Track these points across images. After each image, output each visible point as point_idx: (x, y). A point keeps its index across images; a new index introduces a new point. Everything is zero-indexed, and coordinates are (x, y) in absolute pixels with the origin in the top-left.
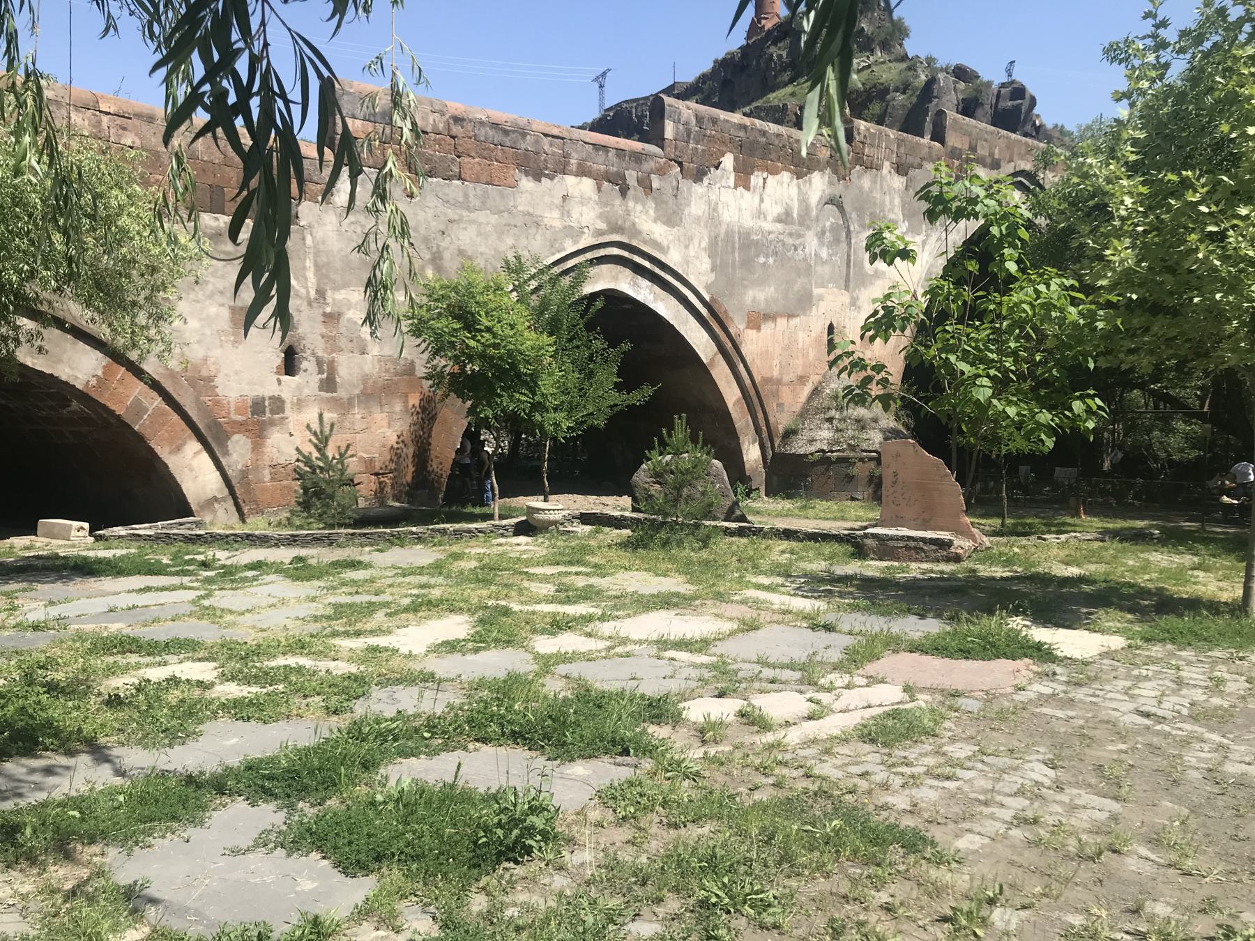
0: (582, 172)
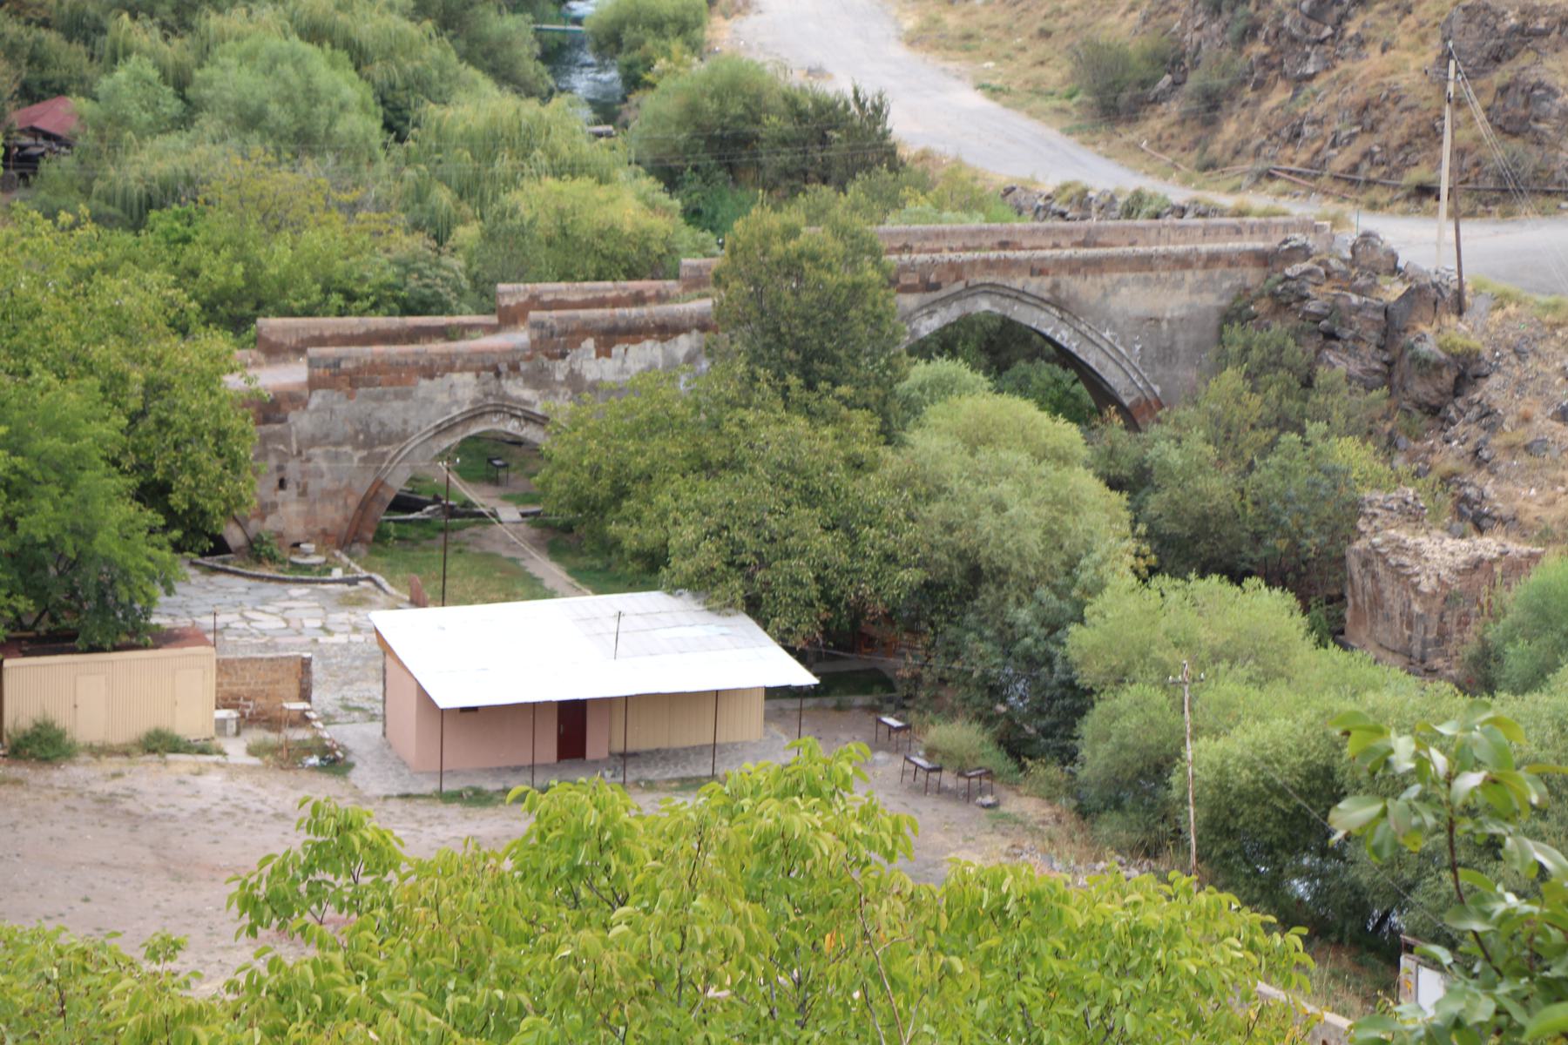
0: (462, 370)
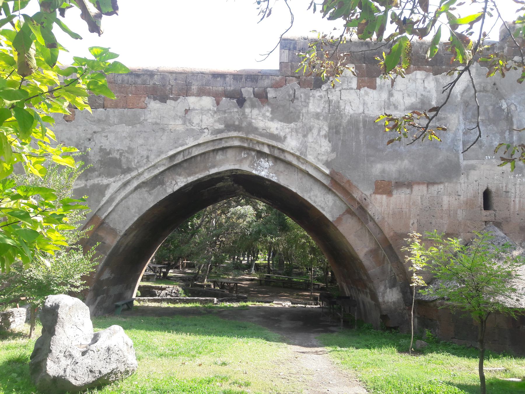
0: (201, 93)
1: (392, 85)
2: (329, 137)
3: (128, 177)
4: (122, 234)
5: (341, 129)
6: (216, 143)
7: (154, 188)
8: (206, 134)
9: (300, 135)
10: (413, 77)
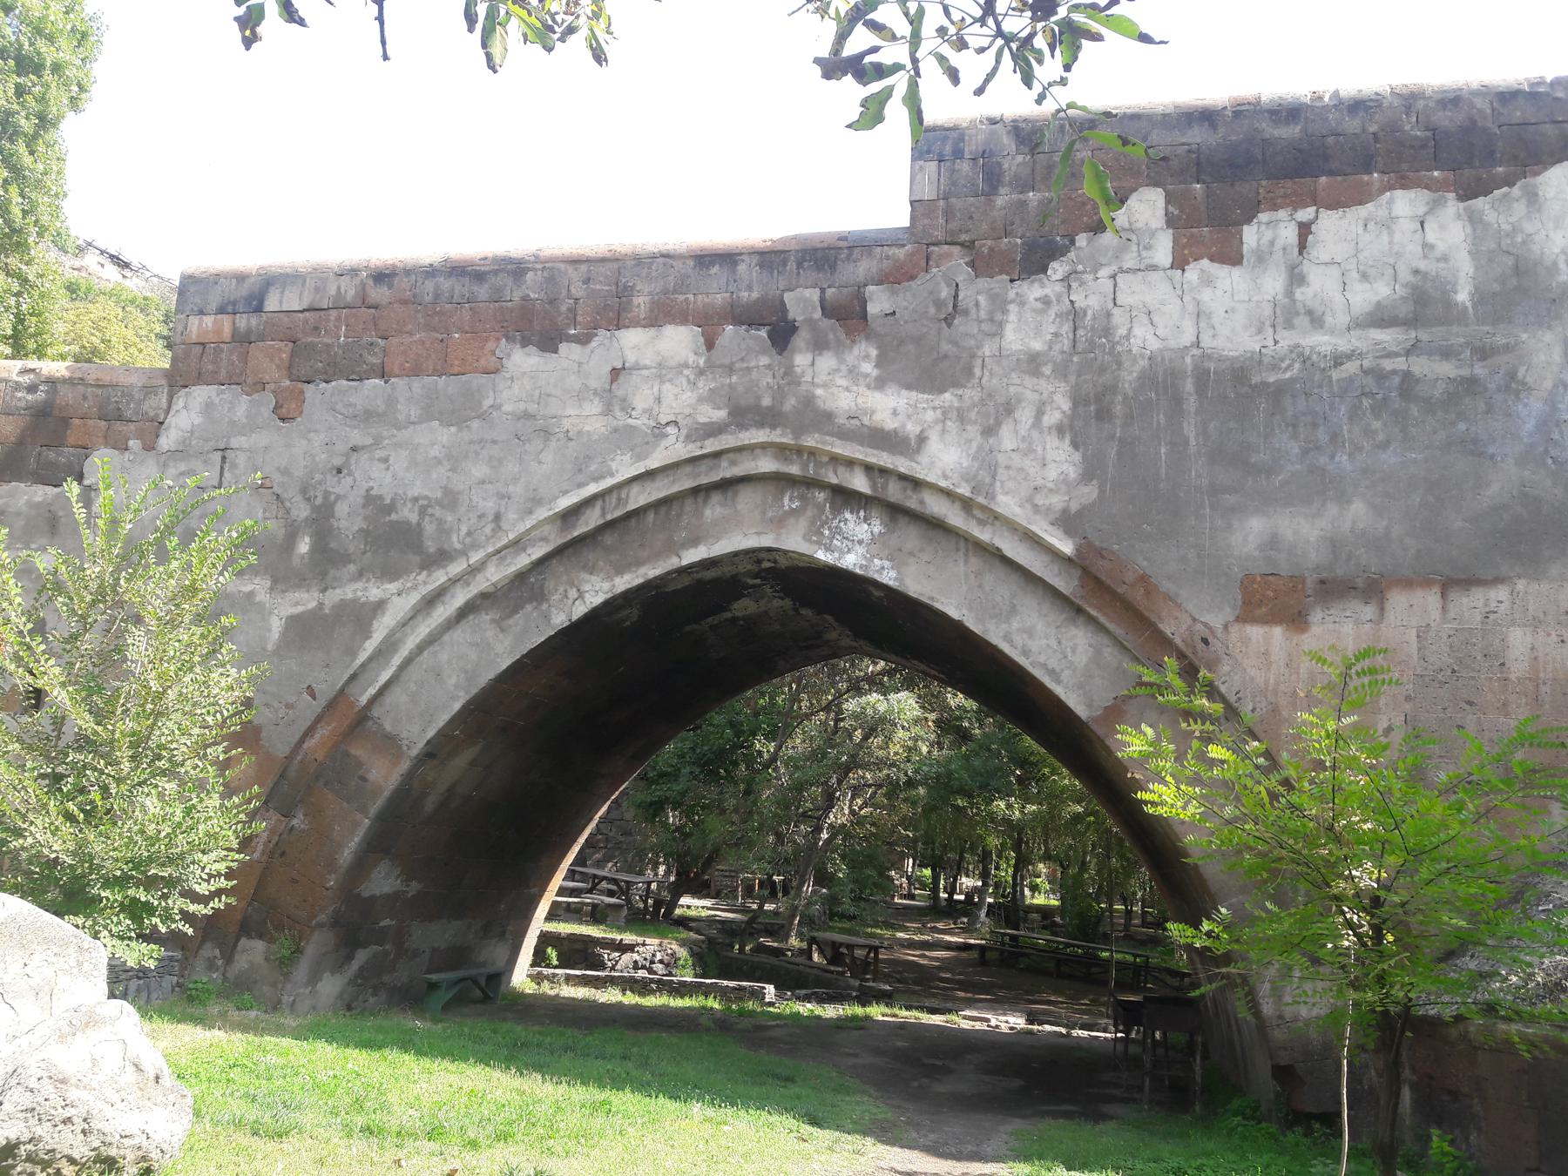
0: (663, 314)
1: (1302, 246)
2: (1070, 430)
3: (440, 577)
4: (415, 752)
5: (1111, 403)
6: (703, 467)
7: (515, 611)
8: (672, 439)
9: (973, 431)
10: (1382, 213)
